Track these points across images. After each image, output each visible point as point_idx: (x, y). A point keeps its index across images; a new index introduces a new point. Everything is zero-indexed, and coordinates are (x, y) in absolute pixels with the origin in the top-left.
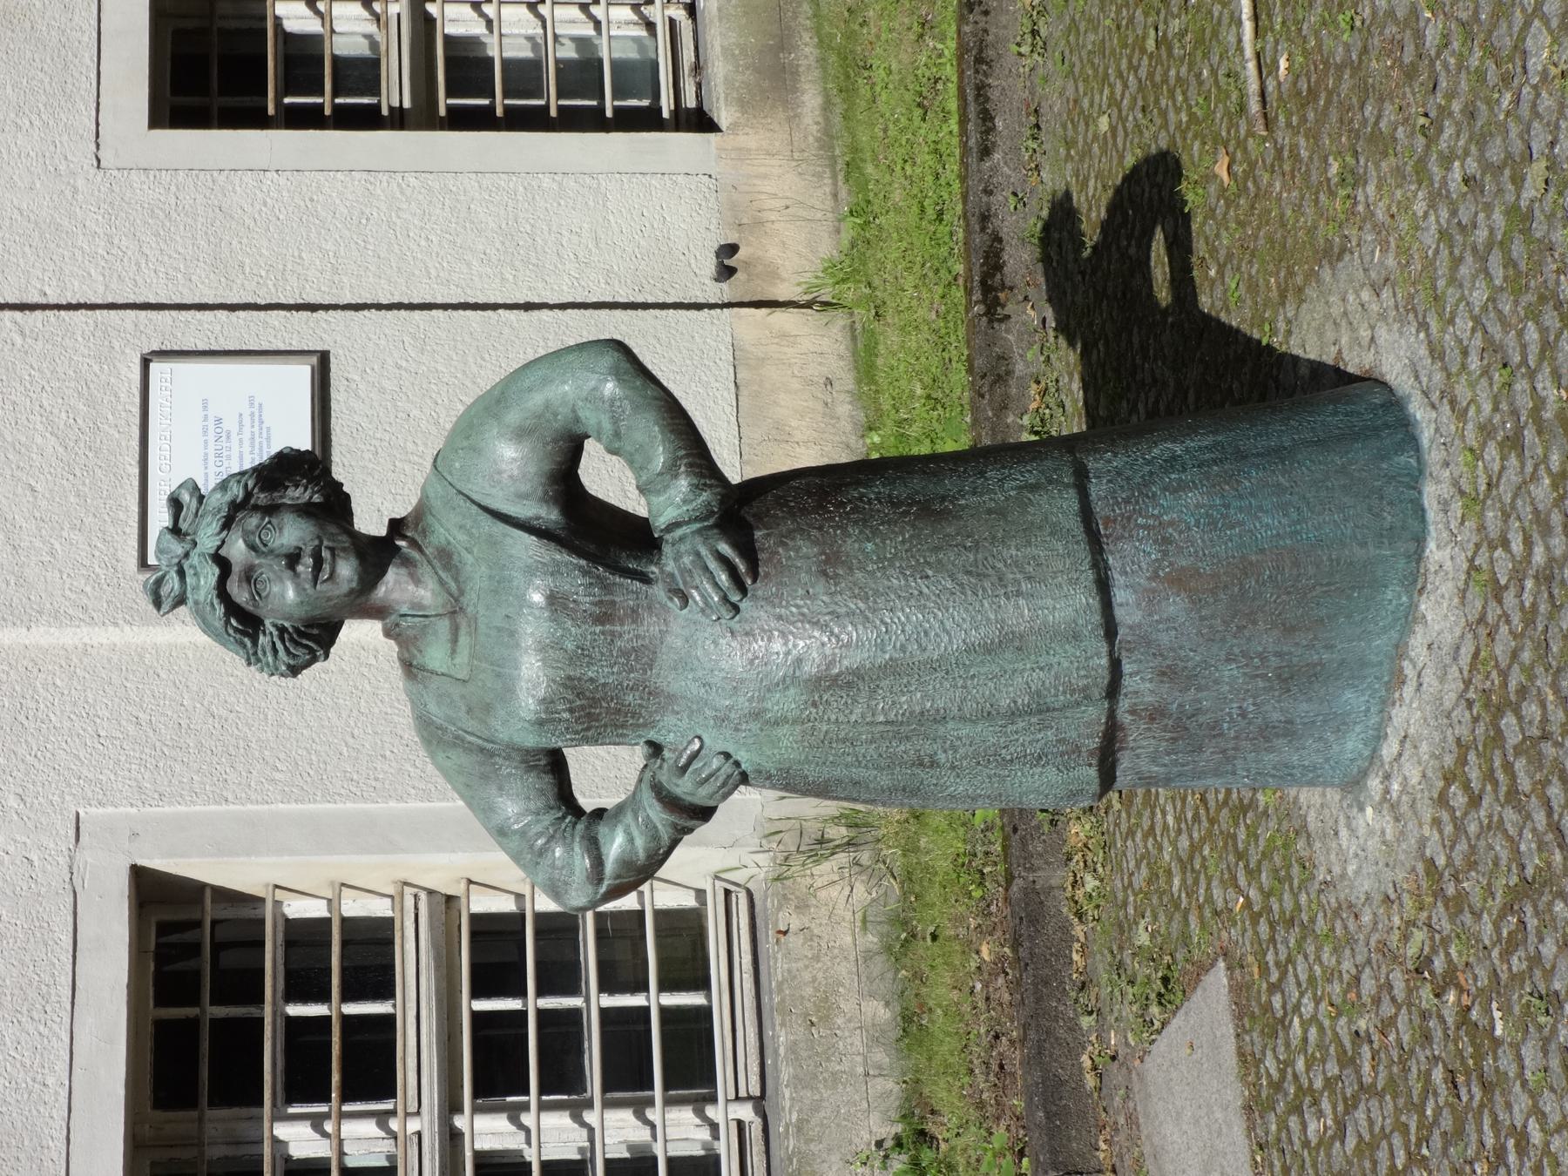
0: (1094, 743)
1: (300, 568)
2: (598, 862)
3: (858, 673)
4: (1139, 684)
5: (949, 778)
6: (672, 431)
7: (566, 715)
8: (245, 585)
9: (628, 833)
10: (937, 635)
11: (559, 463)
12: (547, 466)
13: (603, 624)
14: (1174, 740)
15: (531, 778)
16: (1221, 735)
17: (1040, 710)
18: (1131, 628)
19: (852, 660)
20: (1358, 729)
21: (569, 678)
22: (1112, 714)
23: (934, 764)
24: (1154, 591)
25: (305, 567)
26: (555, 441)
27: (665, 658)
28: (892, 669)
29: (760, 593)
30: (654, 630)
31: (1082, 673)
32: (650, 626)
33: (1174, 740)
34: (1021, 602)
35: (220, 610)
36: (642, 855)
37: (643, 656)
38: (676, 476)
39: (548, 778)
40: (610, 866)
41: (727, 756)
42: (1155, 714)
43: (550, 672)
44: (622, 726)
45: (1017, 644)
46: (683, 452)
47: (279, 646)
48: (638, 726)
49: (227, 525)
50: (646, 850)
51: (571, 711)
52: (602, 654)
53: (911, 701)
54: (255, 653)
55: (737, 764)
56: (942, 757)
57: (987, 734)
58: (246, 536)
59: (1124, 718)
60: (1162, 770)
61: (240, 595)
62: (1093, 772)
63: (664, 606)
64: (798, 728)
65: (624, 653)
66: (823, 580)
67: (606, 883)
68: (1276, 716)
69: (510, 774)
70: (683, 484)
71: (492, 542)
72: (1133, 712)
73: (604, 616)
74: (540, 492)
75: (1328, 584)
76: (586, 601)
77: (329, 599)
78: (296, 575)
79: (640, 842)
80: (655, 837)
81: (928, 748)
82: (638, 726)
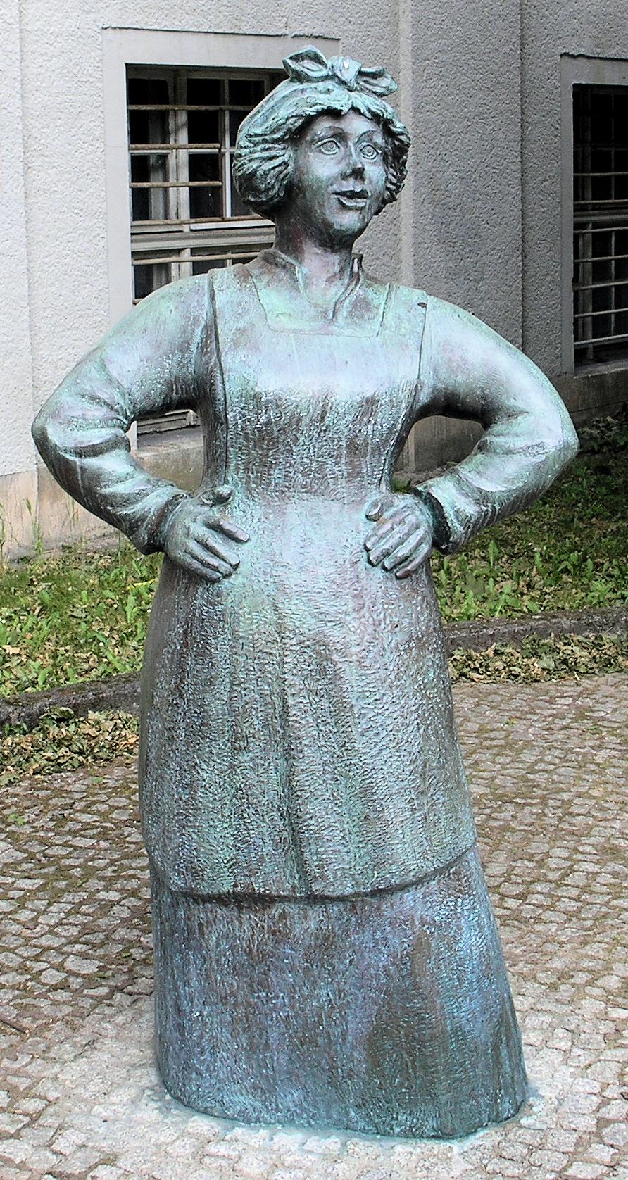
0: (259, 888)
1: (352, 181)
2: (95, 451)
3: (336, 677)
4: (311, 922)
5: (219, 764)
6: (517, 497)
7: (264, 419)
8: (331, 133)
9: (128, 476)
10: (377, 743)
11: (463, 402)
12: (462, 390)
13: (348, 446)
14: (249, 953)
15: (161, 387)
16: (253, 991)
17: (295, 838)
18: (378, 908)
19: (350, 673)
20: (258, 1104)
21: (299, 420)
22: (283, 899)
23: (236, 750)
24: (413, 924)
25: (351, 185)
26: (485, 398)
27: (317, 503)
28: (341, 709)
29: (390, 584)
30: (343, 492)
31: (339, 873)
32: (344, 489)
33: (249, 953)
34: (408, 814)
35: (311, 111)
36: (106, 491)
37: (316, 482)
38: (477, 503)
39: (159, 401)
40: (92, 462)
41: (236, 567)
42: (279, 935)
43: (304, 403)
44: (246, 469)
45: (372, 815)
46: (498, 508)
47: (277, 162)
48: (247, 483)
49: (376, 118)
50: (113, 495)
51: (268, 424)
52: (320, 449)
53: (307, 728)
54: (265, 141)
55: (227, 576)
56: (244, 757)
57: (270, 795)
58: (369, 134)
59: (276, 911)
60: (212, 943)
61: (323, 127)
62: (227, 888)
63: (362, 502)
64: (272, 629)
65: (321, 467)
66: (406, 638)
67: (77, 459)
68: (274, 1035)
69: (163, 368)
70: (471, 510)
71: (403, 346)
72: (283, 916)
73: (355, 448)
74: (440, 385)
75: (414, 1068)
76: (367, 431)
77: (321, 206)
78: (344, 177)
79: (119, 489)
80: (127, 501)
81: (256, 746)
82: (247, 483)
